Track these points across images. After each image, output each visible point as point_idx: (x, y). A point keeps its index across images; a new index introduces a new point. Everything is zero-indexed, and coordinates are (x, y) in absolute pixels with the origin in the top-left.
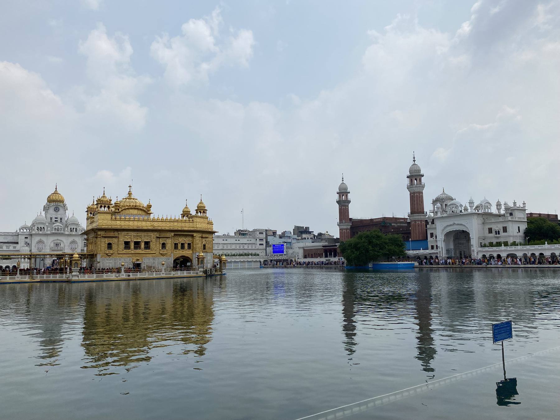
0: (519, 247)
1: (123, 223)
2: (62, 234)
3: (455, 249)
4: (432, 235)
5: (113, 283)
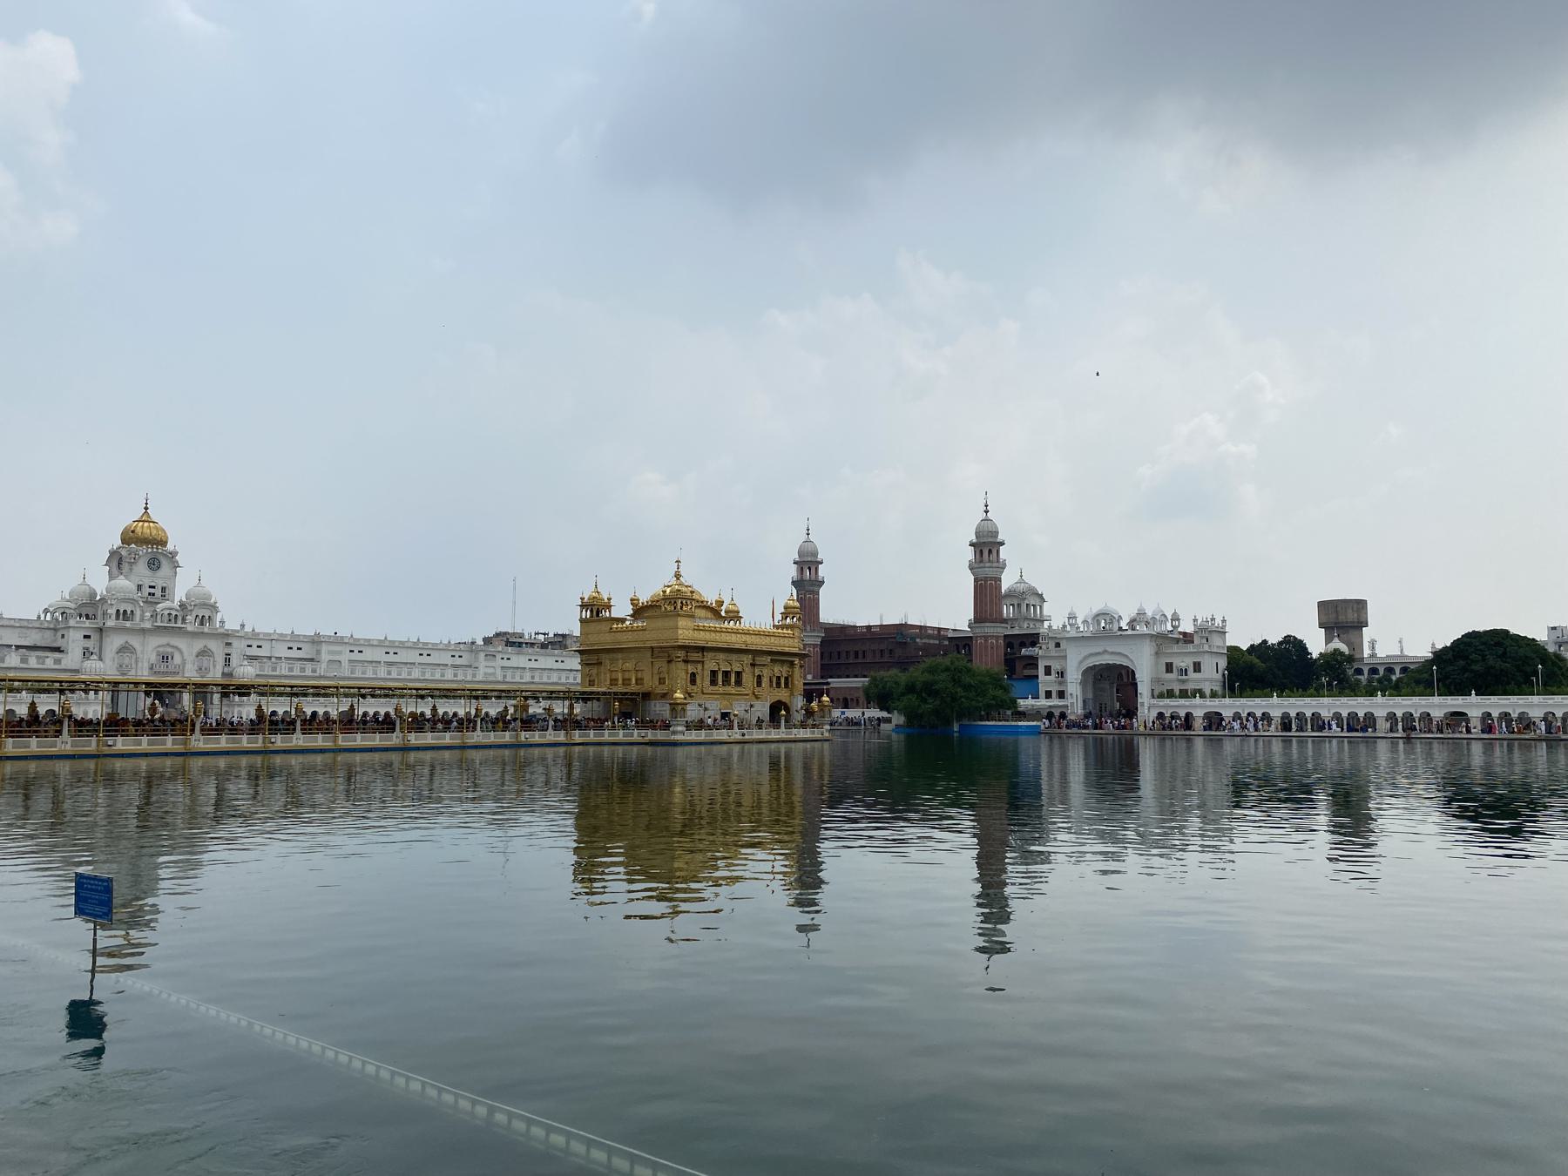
0: (1227, 701)
1: (708, 636)
2: (180, 632)
4: (1048, 671)
5: (725, 747)
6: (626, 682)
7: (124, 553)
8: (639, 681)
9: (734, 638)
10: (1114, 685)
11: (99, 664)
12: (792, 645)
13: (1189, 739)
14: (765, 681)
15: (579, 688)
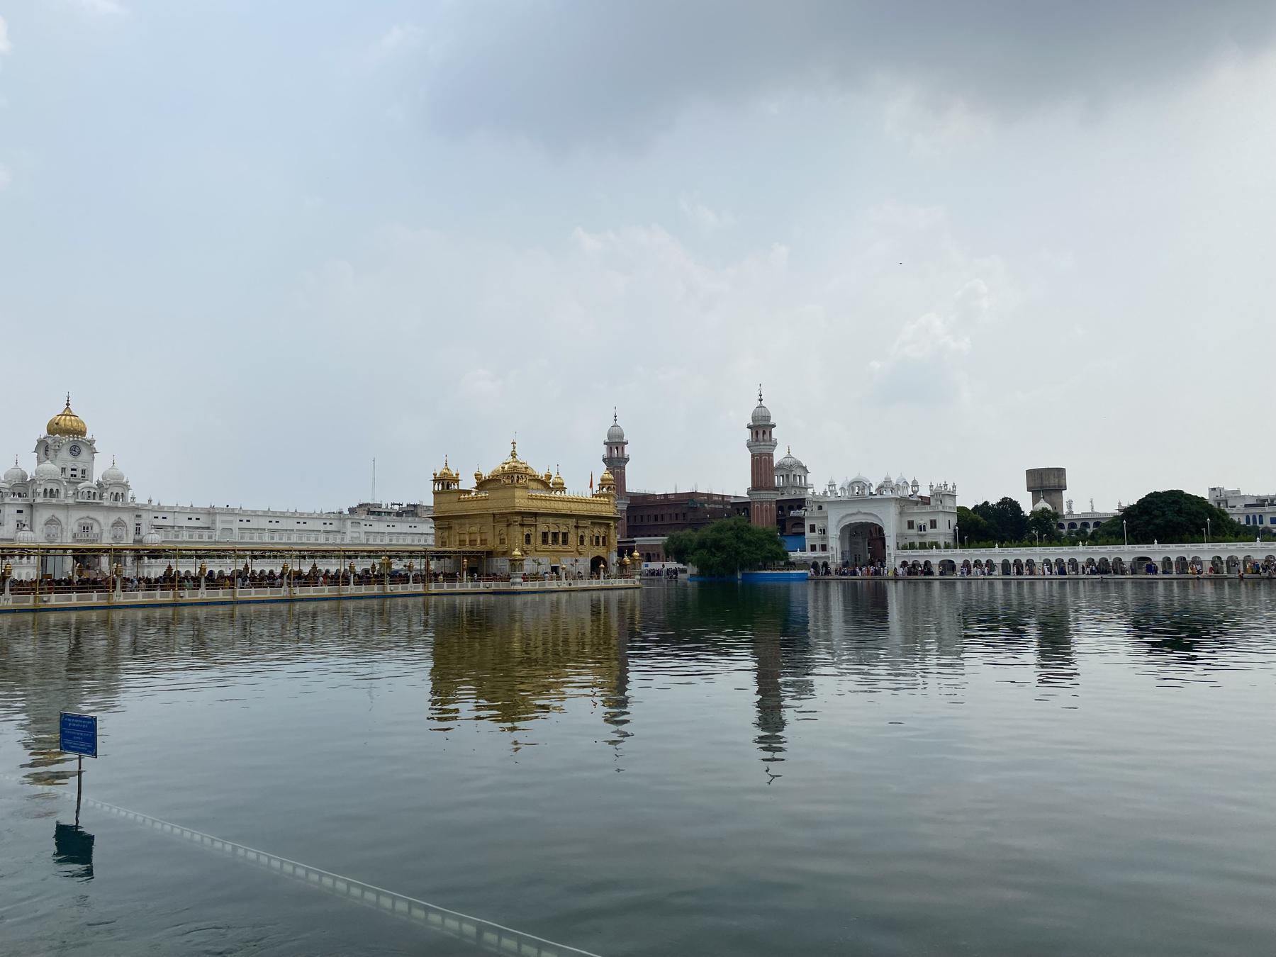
0: (958, 551)
2: (98, 506)
3: (851, 551)
4: (813, 529)
5: (554, 596)
6: (473, 542)
7: (50, 441)
8: (483, 542)
9: (560, 505)
10: (866, 540)
11: (30, 534)
12: (608, 508)
13: (928, 584)
14: (587, 540)
15: (434, 548)
